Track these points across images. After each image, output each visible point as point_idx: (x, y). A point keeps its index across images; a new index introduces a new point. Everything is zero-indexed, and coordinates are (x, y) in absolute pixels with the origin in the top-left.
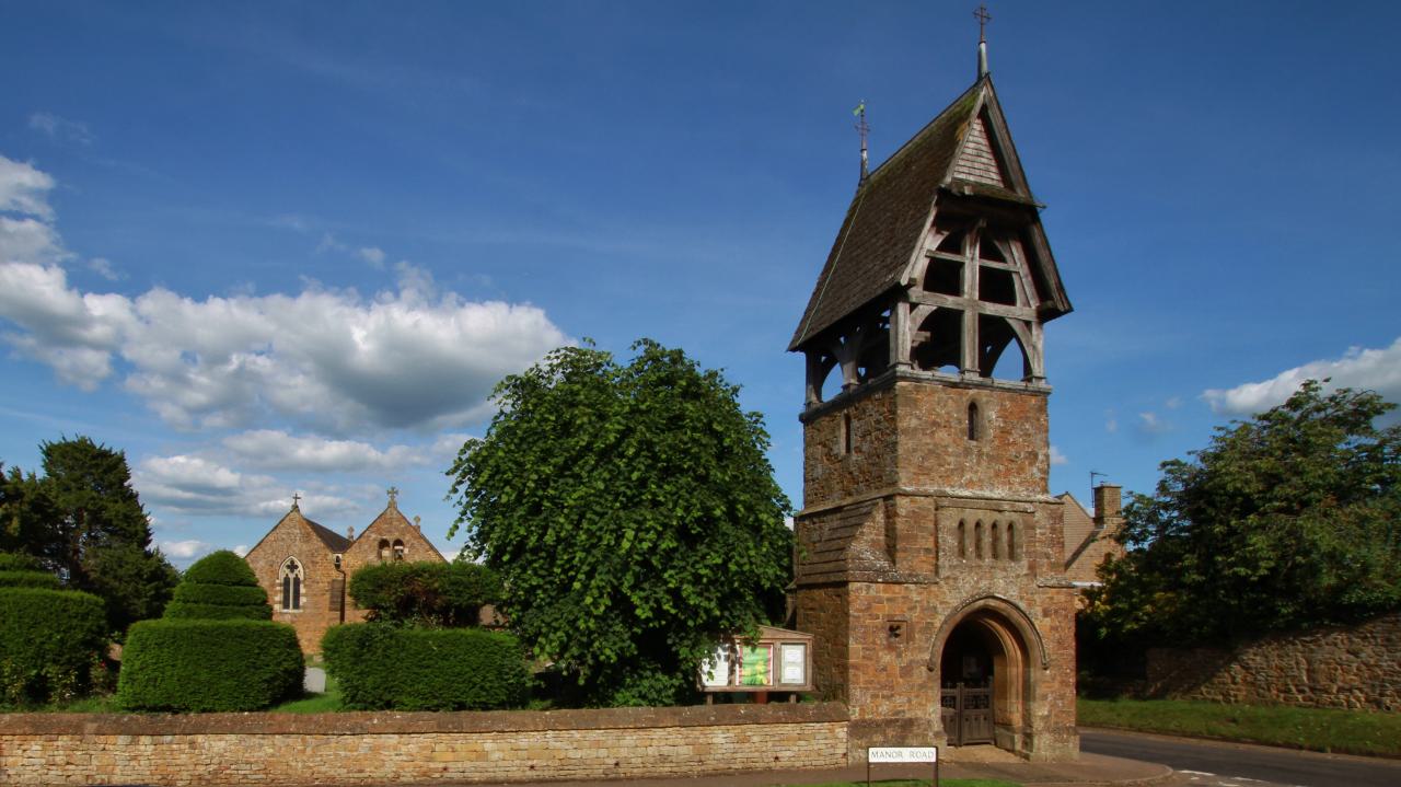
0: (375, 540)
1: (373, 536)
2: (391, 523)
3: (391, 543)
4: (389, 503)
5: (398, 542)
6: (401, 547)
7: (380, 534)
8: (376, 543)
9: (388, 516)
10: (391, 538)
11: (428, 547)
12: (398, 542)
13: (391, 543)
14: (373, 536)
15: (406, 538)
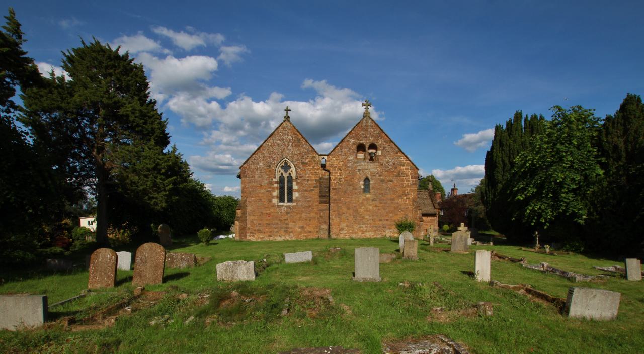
0: (354, 144)
1: (352, 141)
2: (367, 130)
3: (367, 147)
4: (365, 113)
5: (373, 146)
6: (374, 151)
7: (358, 139)
8: (355, 147)
9: (364, 124)
10: (366, 143)
11: (397, 150)
12: (373, 146)
13: (367, 147)
14: (352, 141)
15: (379, 143)
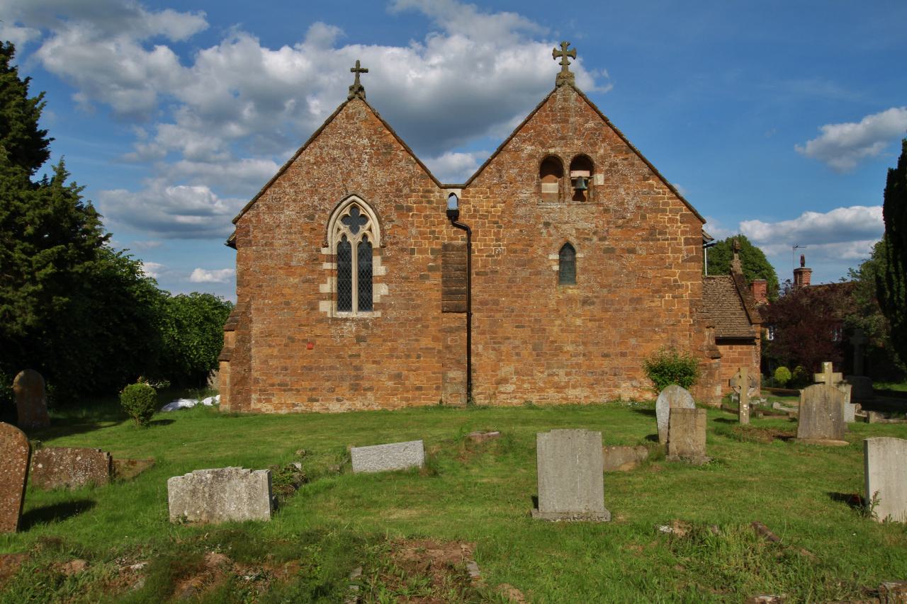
0: (531, 156)
1: (529, 148)
3: (567, 163)
4: (559, 76)
5: (582, 162)
6: (585, 174)
7: (543, 144)
8: (535, 164)
9: (559, 105)
10: (565, 152)
11: (646, 170)
12: (582, 162)
13: (567, 163)
14: (529, 148)
15: (599, 153)
